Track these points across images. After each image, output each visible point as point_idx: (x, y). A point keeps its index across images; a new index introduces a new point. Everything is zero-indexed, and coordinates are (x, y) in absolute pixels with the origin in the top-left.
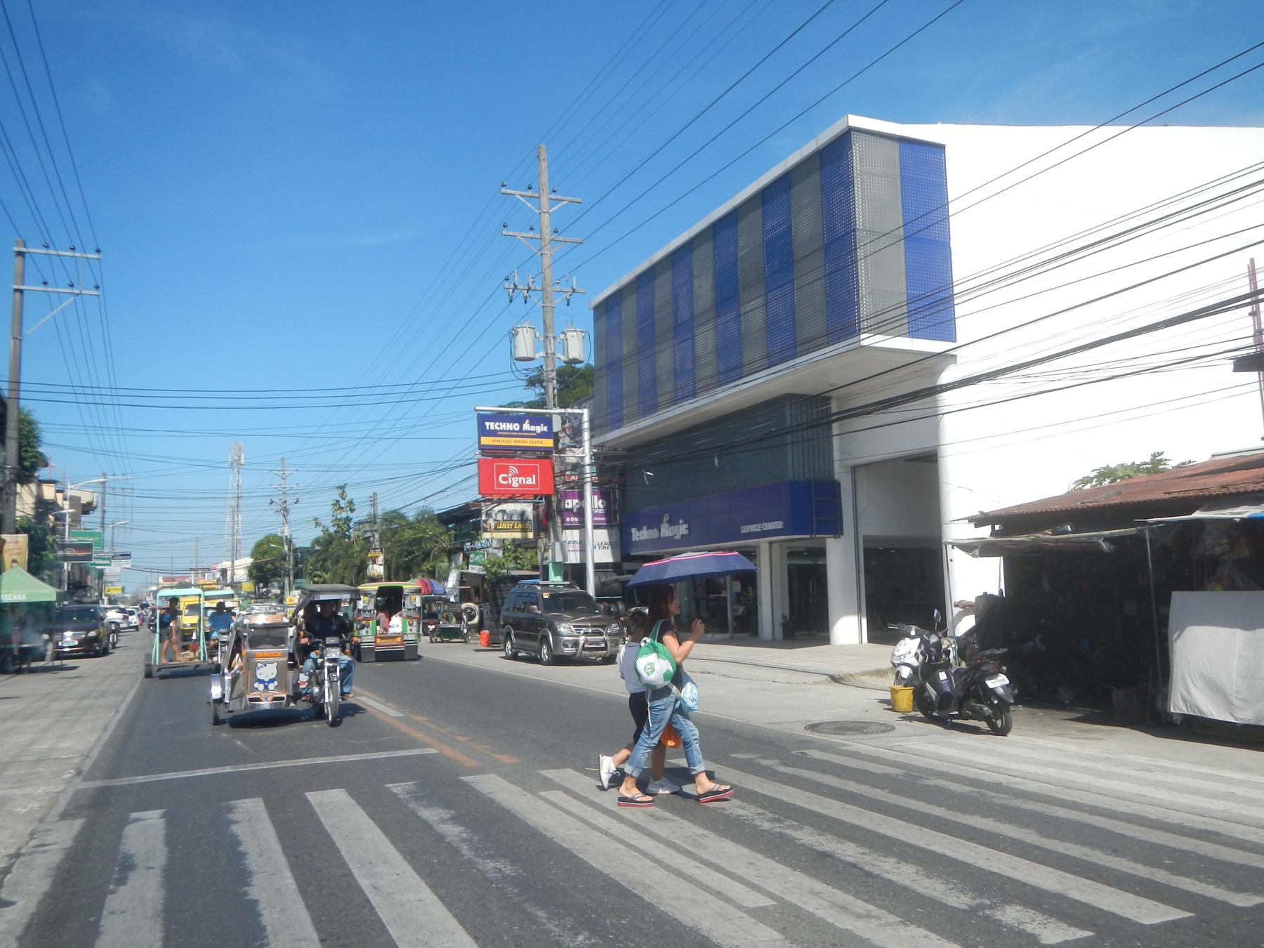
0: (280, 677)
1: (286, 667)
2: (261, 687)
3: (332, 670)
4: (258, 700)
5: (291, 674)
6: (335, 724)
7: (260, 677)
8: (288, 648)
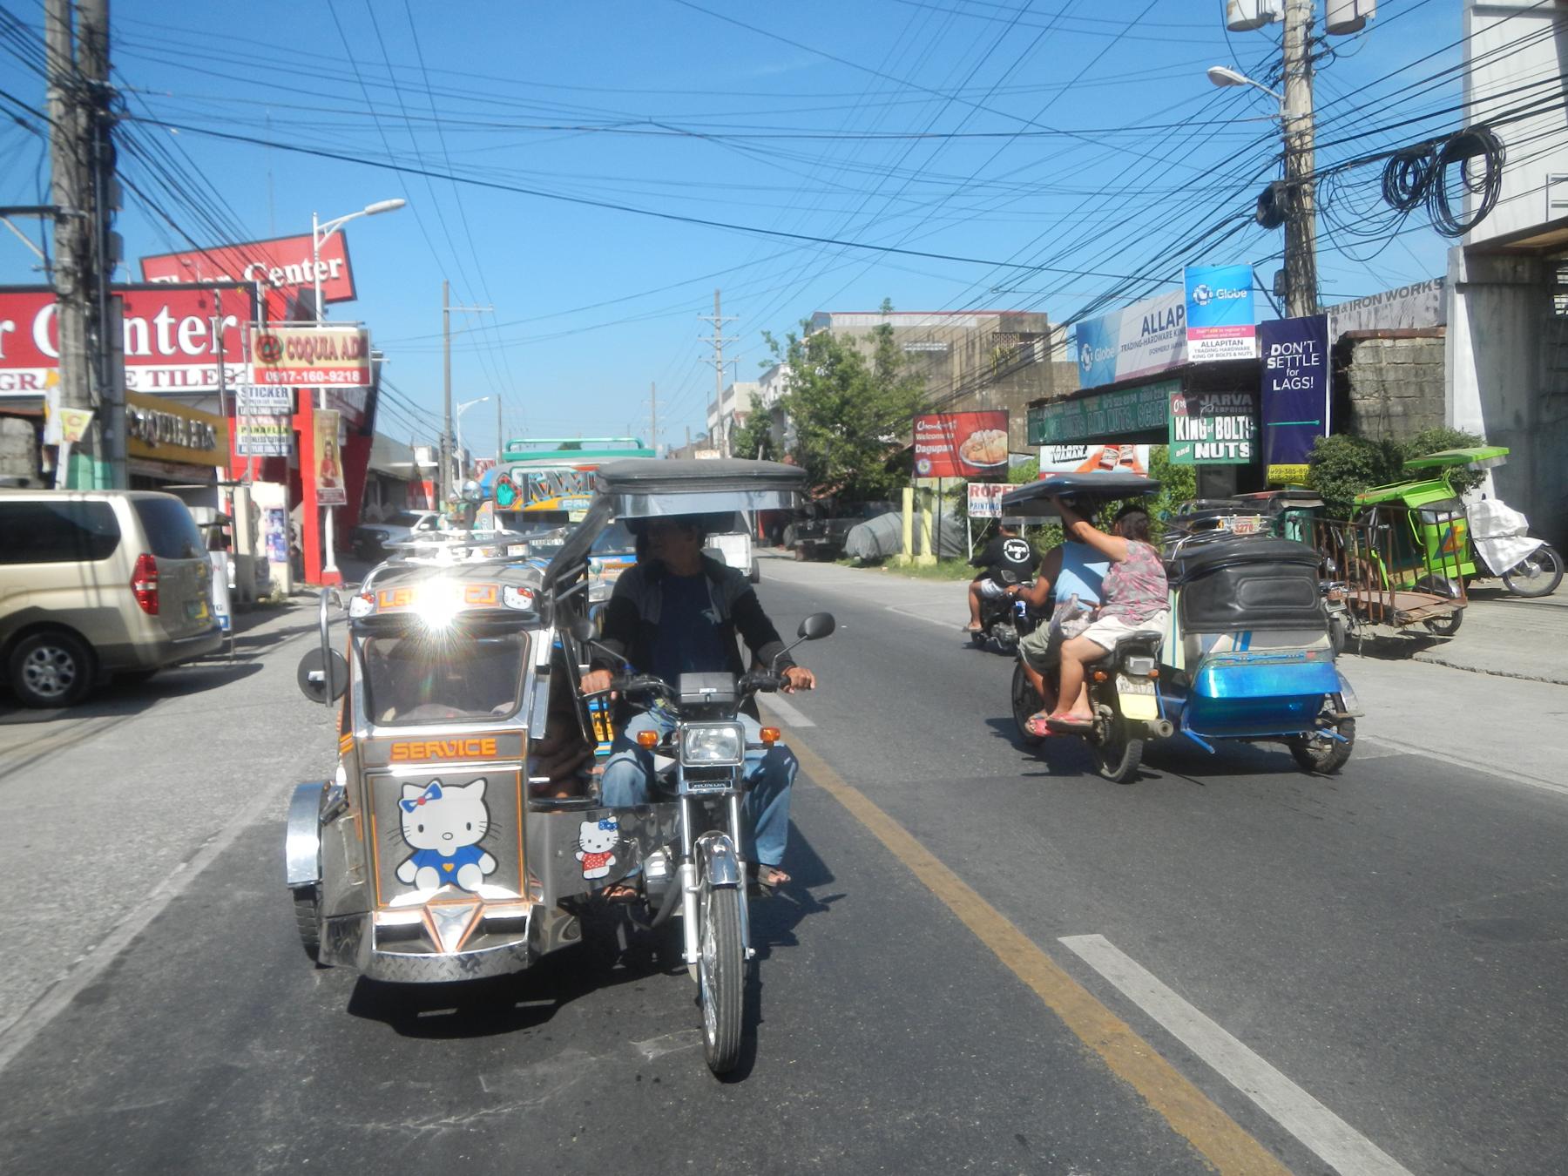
3: (708, 818)
4: (415, 935)
5: (542, 824)
6: (733, 1066)
7: (416, 840)
8: (529, 717)
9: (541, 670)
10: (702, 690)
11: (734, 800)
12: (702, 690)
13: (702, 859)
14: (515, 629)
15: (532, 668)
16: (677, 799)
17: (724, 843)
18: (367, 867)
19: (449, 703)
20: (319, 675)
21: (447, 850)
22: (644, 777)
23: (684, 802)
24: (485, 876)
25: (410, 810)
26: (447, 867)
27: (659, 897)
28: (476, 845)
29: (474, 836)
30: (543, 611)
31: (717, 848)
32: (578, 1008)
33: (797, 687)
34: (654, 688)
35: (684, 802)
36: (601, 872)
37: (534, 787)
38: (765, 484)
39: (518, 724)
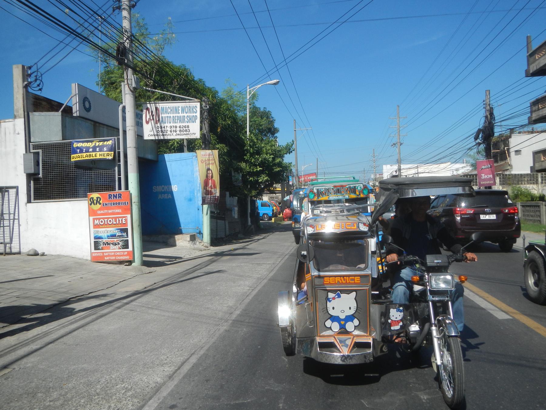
0: (361, 314)
1: (369, 299)
2: (336, 327)
3: (441, 309)
5: (375, 310)
7: (332, 312)
9: (374, 253)
10: (436, 261)
11: (450, 303)
12: (436, 261)
13: (440, 324)
14: (362, 238)
15: (370, 252)
16: (427, 302)
17: (449, 319)
18: (314, 321)
19: (341, 264)
20: (305, 253)
21: (342, 316)
22: (408, 292)
23: (430, 303)
24: (355, 326)
25: (330, 301)
26: (342, 322)
27: (415, 338)
28: (352, 315)
29: (352, 312)
30: (372, 232)
31: (447, 321)
32: (385, 378)
33: (470, 260)
34: (415, 260)
35: (430, 303)
36: (397, 327)
37: (373, 295)
38: (457, 184)
39: (368, 272)
